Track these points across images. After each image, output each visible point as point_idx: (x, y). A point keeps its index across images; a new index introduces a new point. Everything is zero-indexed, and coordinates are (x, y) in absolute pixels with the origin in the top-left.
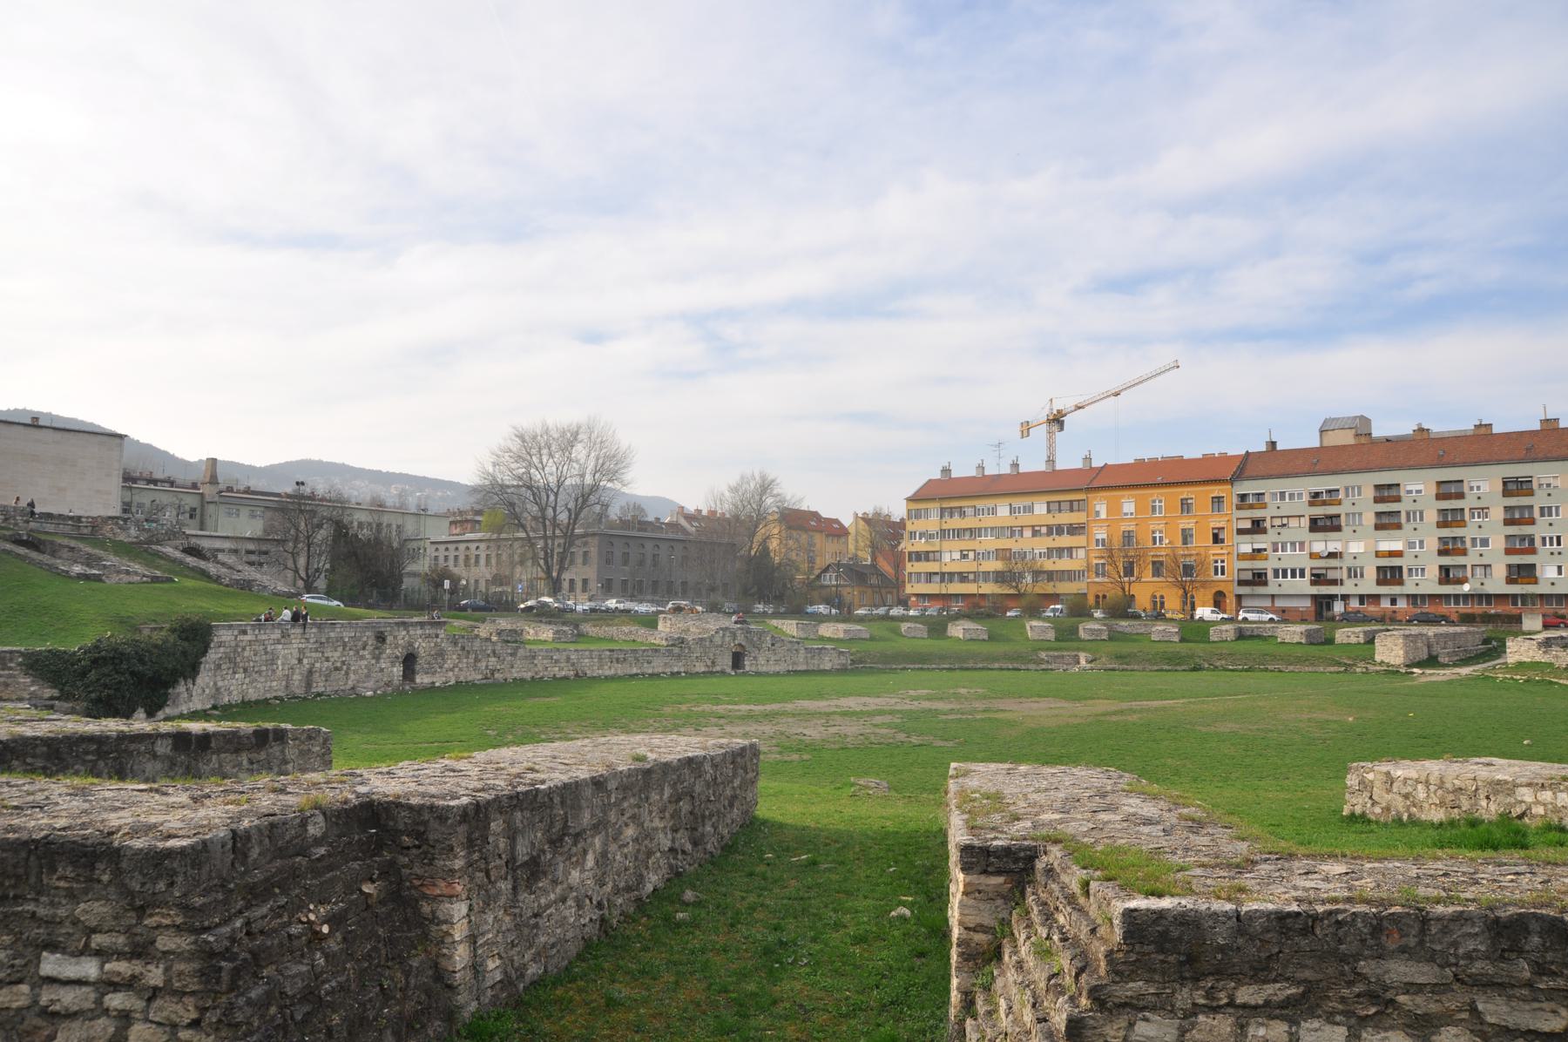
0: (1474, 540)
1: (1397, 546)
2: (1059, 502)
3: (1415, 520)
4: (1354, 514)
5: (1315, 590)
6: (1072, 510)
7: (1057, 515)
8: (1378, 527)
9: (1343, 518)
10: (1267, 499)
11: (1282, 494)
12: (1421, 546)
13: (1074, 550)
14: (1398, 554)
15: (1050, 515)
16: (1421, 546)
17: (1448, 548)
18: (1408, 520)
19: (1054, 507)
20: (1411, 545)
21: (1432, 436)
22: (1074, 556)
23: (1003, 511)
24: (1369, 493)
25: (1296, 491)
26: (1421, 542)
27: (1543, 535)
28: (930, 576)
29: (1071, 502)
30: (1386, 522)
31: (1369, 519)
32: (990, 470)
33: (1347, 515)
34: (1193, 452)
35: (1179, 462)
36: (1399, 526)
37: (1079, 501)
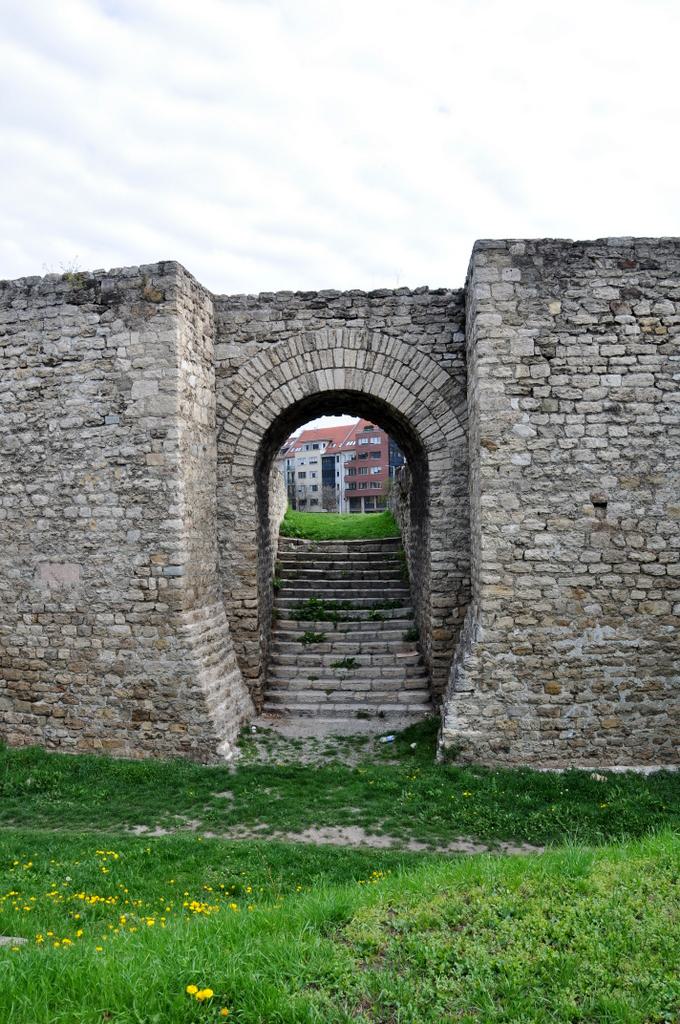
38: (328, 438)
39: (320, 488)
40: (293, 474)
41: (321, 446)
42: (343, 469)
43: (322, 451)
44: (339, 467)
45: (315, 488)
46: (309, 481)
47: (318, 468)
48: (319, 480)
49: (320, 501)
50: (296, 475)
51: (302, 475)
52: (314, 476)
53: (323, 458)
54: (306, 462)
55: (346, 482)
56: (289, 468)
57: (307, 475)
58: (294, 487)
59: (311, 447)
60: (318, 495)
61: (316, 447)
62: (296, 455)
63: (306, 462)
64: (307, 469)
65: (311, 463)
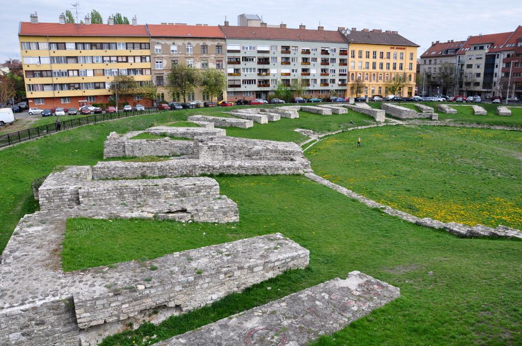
0: (244, 69)
1: (288, 71)
2: (133, 43)
3: (294, 61)
4: (274, 58)
5: (259, 89)
6: (141, 48)
7: (133, 51)
8: (282, 63)
9: (270, 59)
10: (291, 49)
11: (247, 48)
12: (296, 72)
13: (144, 70)
14: (289, 74)
15: (128, 51)
16: (296, 72)
17: (305, 71)
18: (292, 61)
19: (130, 46)
20: (293, 71)
21: (268, 27)
22: (144, 73)
23: (70, 46)
24: (280, 49)
25: (253, 46)
26: (296, 70)
27: (293, 69)
28: (43, 86)
29: (141, 44)
30: (286, 62)
31: (279, 60)
32: (41, 20)
33: (272, 58)
34: (192, 23)
35: (183, 27)
36: (289, 63)
37: (145, 43)
38: (491, 42)
39: (482, 75)
40: (462, 65)
41: (486, 47)
42: (502, 63)
43: (486, 50)
44: (500, 62)
45: (478, 75)
46: (475, 70)
47: (482, 63)
48: (482, 71)
49: (481, 84)
50: (465, 67)
51: (470, 66)
52: (478, 67)
53: (486, 55)
54: (474, 58)
55: (502, 72)
56: (459, 61)
57: (473, 66)
58: (461, 74)
59: (478, 48)
60: (481, 80)
61: (482, 48)
62: (466, 53)
63: (474, 58)
64: (474, 62)
65: (477, 58)
